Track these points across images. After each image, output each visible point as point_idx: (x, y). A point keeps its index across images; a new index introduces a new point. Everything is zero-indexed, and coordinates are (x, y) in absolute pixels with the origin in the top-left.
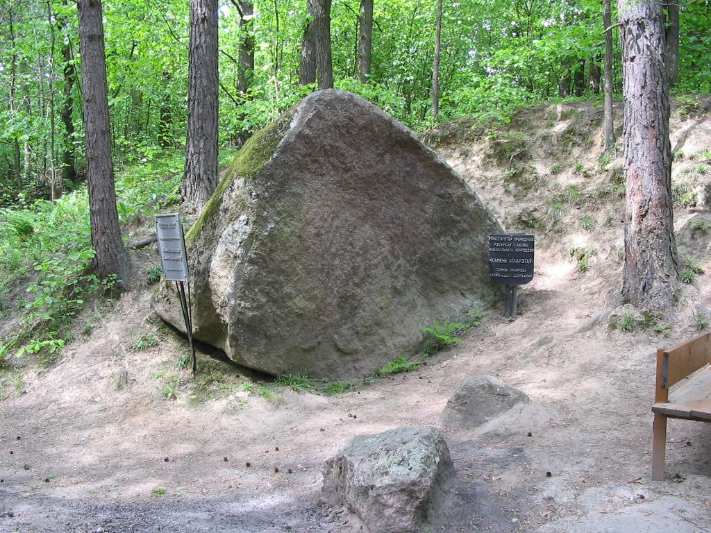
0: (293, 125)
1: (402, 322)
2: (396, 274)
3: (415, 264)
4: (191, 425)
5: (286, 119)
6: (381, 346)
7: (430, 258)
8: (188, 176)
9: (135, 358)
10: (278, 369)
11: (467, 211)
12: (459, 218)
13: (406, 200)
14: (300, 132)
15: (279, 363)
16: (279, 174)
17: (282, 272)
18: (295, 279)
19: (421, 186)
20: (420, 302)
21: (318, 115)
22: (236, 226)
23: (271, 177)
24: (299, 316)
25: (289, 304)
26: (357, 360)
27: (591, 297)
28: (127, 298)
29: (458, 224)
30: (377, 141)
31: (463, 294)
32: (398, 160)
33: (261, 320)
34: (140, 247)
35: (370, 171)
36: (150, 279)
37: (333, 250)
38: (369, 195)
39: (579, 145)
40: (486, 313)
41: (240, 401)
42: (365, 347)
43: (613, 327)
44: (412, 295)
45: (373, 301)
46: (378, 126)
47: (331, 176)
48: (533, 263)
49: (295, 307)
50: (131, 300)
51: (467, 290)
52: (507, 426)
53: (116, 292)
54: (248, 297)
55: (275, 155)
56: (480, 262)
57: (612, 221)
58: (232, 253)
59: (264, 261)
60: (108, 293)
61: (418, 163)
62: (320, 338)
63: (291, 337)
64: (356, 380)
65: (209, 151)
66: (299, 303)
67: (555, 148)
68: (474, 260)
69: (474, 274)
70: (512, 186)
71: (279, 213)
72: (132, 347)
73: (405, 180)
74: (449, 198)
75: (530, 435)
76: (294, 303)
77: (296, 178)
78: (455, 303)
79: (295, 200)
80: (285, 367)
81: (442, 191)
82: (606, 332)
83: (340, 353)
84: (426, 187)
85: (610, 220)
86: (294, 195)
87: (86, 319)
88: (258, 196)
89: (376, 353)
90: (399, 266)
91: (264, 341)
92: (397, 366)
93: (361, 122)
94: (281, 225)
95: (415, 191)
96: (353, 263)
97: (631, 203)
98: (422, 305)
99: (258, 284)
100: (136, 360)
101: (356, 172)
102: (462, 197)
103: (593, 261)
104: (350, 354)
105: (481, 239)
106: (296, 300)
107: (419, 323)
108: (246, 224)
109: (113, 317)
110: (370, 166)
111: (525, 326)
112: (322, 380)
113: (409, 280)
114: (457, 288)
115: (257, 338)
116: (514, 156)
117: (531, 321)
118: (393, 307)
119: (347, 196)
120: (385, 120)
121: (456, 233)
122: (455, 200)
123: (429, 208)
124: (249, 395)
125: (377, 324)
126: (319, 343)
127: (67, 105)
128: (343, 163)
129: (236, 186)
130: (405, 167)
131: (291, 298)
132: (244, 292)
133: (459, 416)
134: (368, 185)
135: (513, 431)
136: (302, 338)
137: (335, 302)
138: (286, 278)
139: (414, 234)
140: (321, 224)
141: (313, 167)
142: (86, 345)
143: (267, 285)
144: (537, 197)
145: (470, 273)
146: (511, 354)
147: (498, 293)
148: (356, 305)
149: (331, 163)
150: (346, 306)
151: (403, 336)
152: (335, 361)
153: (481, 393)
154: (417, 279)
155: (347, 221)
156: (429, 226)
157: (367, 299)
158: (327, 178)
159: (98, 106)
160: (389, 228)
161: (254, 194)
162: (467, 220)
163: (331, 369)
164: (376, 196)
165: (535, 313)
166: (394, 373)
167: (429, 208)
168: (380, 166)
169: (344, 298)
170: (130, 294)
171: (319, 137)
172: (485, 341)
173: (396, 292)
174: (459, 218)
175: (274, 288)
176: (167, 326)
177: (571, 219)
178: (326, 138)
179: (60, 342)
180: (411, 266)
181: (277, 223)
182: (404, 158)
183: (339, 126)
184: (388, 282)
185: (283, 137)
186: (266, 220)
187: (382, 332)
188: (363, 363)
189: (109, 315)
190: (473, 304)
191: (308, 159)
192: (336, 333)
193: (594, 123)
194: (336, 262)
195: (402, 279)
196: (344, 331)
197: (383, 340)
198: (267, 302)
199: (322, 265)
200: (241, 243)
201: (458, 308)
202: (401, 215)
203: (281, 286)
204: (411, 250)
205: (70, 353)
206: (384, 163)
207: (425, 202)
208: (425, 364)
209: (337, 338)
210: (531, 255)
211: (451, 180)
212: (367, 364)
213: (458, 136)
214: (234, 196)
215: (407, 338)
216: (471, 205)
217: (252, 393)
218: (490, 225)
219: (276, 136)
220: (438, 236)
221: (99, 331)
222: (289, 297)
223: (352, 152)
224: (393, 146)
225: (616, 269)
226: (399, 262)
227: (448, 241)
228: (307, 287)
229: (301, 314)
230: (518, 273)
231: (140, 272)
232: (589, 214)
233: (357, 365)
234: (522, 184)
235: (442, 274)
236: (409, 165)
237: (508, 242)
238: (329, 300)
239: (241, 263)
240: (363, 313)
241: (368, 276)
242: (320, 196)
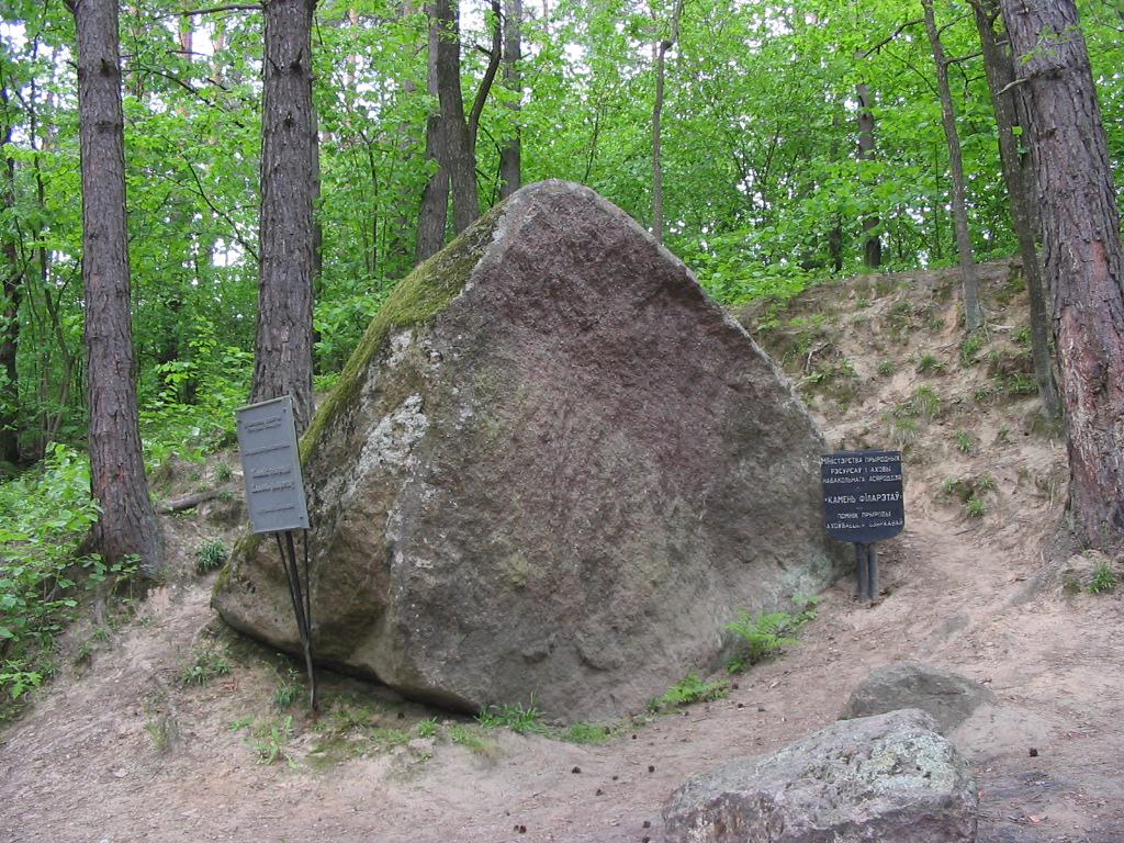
0: (498, 235)
1: (688, 611)
2: (672, 523)
3: (701, 507)
4: (326, 804)
5: (482, 228)
6: (657, 656)
7: (726, 496)
8: (260, 392)
9: (189, 698)
10: (482, 694)
11: (779, 414)
12: (767, 428)
13: (682, 391)
14: (511, 248)
15: (484, 682)
16: (477, 321)
17: (486, 503)
18: (511, 518)
19: (706, 367)
20: (712, 576)
21: (541, 221)
22: (401, 416)
23: (462, 325)
24: (520, 589)
25: (502, 565)
26: (614, 683)
27: (1007, 553)
28: (159, 599)
29: (766, 438)
30: (634, 279)
31: (780, 564)
32: (666, 318)
33: (452, 594)
34: (179, 509)
35: (624, 333)
36: (201, 565)
37: (569, 471)
38: (622, 376)
39: (918, 329)
40: (821, 597)
41: (419, 755)
42: (630, 657)
43: (1072, 589)
44: (698, 563)
45: (639, 569)
46: (636, 252)
47: (561, 336)
48: (901, 500)
49: (513, 572)
50: (167, 601)
51: (788, 556)
52: (976, 747)
53: (141, 585)
54: (429, 549)
55: (469, 286)
56: (806, 506)
57: (1008, 436)
59: (457, 481)
60: (123, 588)
61: (698, 327)
62: (552, 638)
63: (506, 630)
64: (617, 721)
65: (298, 347)
66: (518, 565)
68: (796, 502)
69: (798, 527)
70: (818, 399)
71: (478, 393)
72: (180, 678)
73: (678, 354)
74: (749, 391)
75: (1034, 753)
76: (510, 564)
77: (505, 333)
78: (770, 581)
79: (504, 372)
80: (493, 693)
81: (738, 379)
82: (1061, 601)
83: (584, 668)
84: (712, 369)
85: (1002, 435)
86: (505, 362)
87: (80, 633)
88: (441, 357)
89: (647, 667)
90: (676, 509)
91: (456, 638)
92: (688, 691)
93: (609, 242)
94: (484, 414)
95: (696, 376)
96: (603, 498)
97: (1074, 373)
98: (716, 584)
99: (445, 525)
100: (190, 702)
101: (600, 333)
102: (770, 391)
103: (990, 500)
104: (604, 670)
105: (805, 465)
106: (514, 559)
107: (714, 618)
108: (420, 412)
109: (135, 632)
110: (622, 324)
111: (905, 608)
112: (556, 722)
113: (692, 536)
114: (771, 553)
115: (445, 632)
116: (814, 354)
117: (912, 599)
118: (672, 583)
119: (586, 377)
120: (647, 243)
121: (763, 455)
122: (760, 394)
123: (720, 407)
124: (434, 744)
125: (647, 613)
126: (552, 646)
127: (10, 336)
128: (579, 314)
129: (394, 347)
130: (679, 330)
131: (504, 555)
132: (420, 540)
134: (624, 358)
135: (994, 753)
136: (523, 635)
137: (576, 568)
138: (495, 515)
139: (697, 452)
140: (548, 418)
141: (533, 313)
142: (84, 684)
143: (462, 527)
144: (865, 413)
145: (791, 527)
146: (900, 652)
147: (839, 562)
148: (611, 576)
149: (560, 312)
150: (595, 577)
151: (692, 637)
152: (578, 683)
153: (902, 693)
154: (706, 536)
155: (589, 420)
156: (720, 440)
157: (628, 567)
158: (554, 339)
159: (111, 245)
160: (656, 440)
161: (434, 354)
162: (782, 431)
163: (571, 699)
164: (634, 381)
165: (916, 587)
166: (685, 704)
167: (720, 407)
168: (639, 325)
169: (591, 563)
170: (164, 590)
171: (542, 260)
172: (836, 640)
173: (676, 556)
174: (767, 428)
175: (473, 532)
176: (247, 641)
177: (933, 440)
178: (553, 264)
179: (33, 676)
180: (695, 511)
181: (476, 409)
182: (676, 315)
183: (573, 244)
184: (661, 537)
185: (481, 256)
186: (456, 402)
187: (658, 629)
188: (626, 689)
189: (126, 629)
190: (799, 581)
191: (523, 298)
192: (579, 628)
193: (939, 293)
194: (575, 495)
195: (682, 532)
196: (592, 626)
197: (659, 643)
198: (462, 560)
199: (554, 497)
200: (411, 445)
201: (776, 590)
202: (674, 417)
203: (487, 531)
204: (694, 481)
205: (52, 701)
206: (645, 321)
207: (713, 395)
208: (736, 687)
209: (582, 639)
210: (898, 487)
211: (753, 358)
212: (635, 690)
214: (392, 365)
215: (698, 642)
216: (785, 405)
217: (441, 739)
218: (815, 442)
219: (467, 257)
220: (736, 456)
221: (107, 656)
222: (500, 551)
223: (596, 295)
224: (659, 291)
225: (1038, 507)
226: (676, 502)
227: (753, 468)
228: (530, 536)
229: (522, 587)
230: (878, 519)
231: (181, 554)
232: (964, 430)
233: (616, 692)
234: (832, 395)
235: (745, 526)
236: (684, 328)
237: (856, 466)
238: (565, 565)
239: (414, 483)
240: (623, 592)
241: (628, 525)
242: (545, 369)
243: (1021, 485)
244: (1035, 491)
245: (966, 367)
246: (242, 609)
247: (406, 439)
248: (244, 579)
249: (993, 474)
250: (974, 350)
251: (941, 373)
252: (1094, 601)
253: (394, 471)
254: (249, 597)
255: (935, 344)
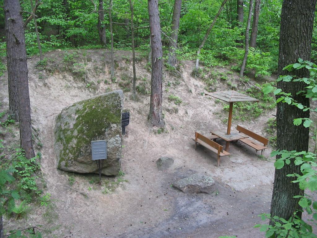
58: (118, 147)
67: (94, 74)
70: (90, 89)
85: (126, 99)
133: (164, 167)
210: (129, 118)
213: (58, 69)
243: (134, 110)
244: (137, 112)
245: (113, 83)
246: (74, 169)
247: (119, 142)
248: (74, 164)
249: (129, 108)
250: (115, 80)
251: (109, 84)
252: (159, 135)
253: (118, 147)
254: (75, 167)
255: (106, 77)
